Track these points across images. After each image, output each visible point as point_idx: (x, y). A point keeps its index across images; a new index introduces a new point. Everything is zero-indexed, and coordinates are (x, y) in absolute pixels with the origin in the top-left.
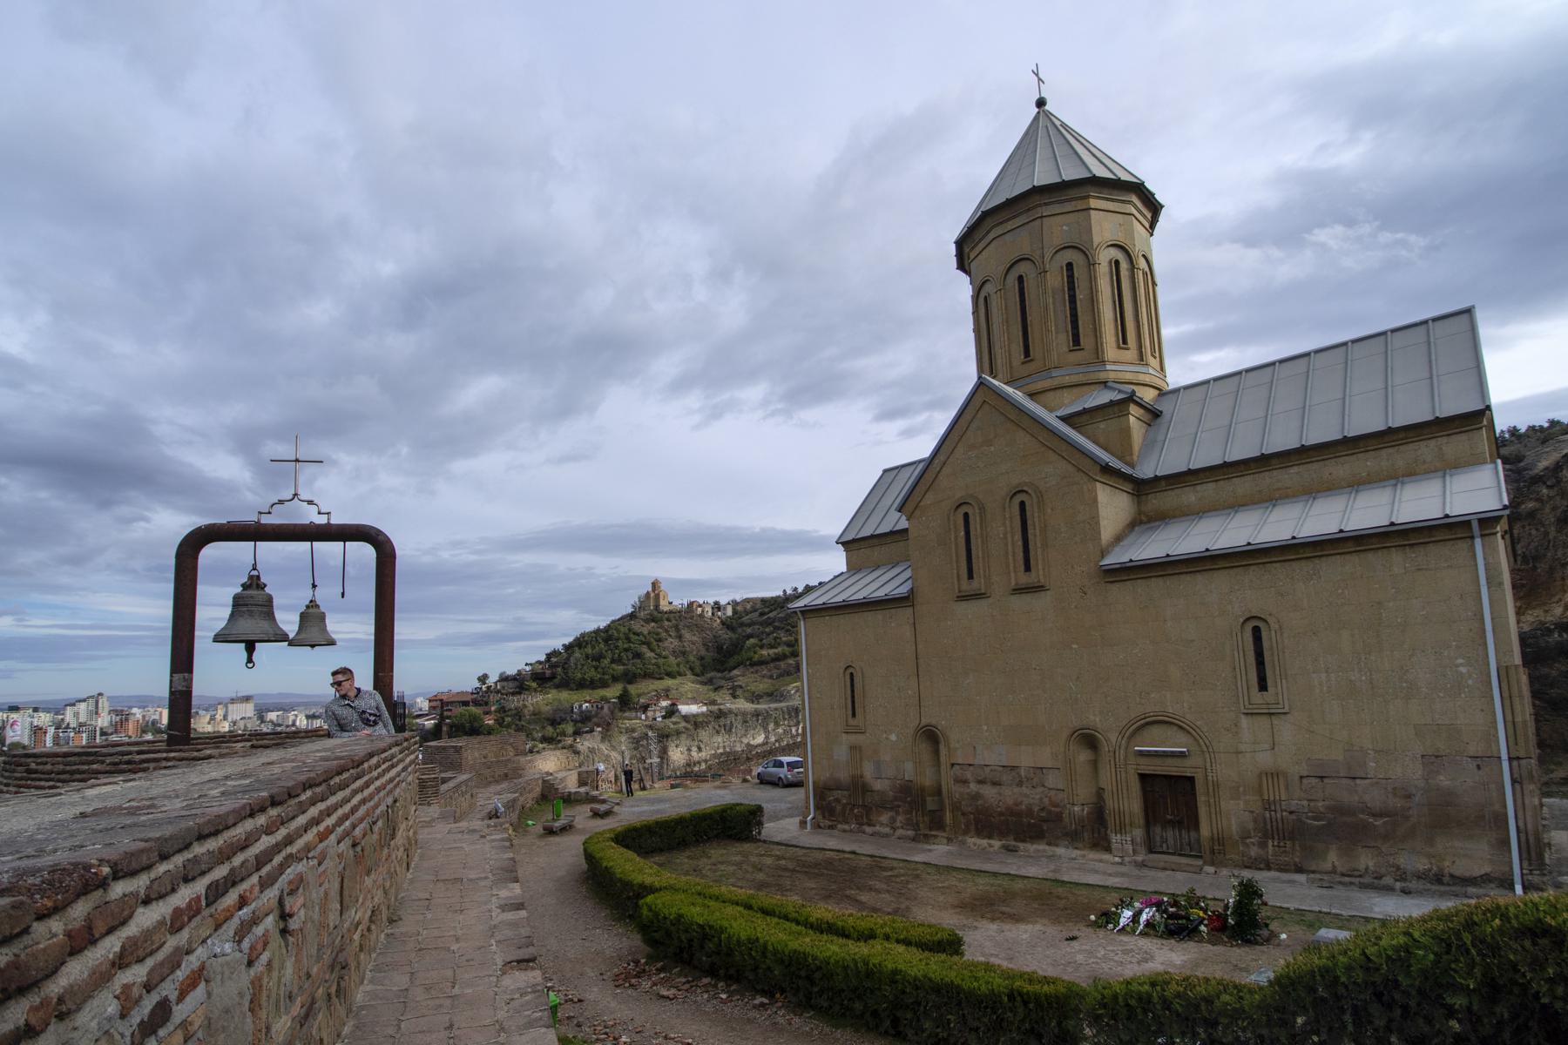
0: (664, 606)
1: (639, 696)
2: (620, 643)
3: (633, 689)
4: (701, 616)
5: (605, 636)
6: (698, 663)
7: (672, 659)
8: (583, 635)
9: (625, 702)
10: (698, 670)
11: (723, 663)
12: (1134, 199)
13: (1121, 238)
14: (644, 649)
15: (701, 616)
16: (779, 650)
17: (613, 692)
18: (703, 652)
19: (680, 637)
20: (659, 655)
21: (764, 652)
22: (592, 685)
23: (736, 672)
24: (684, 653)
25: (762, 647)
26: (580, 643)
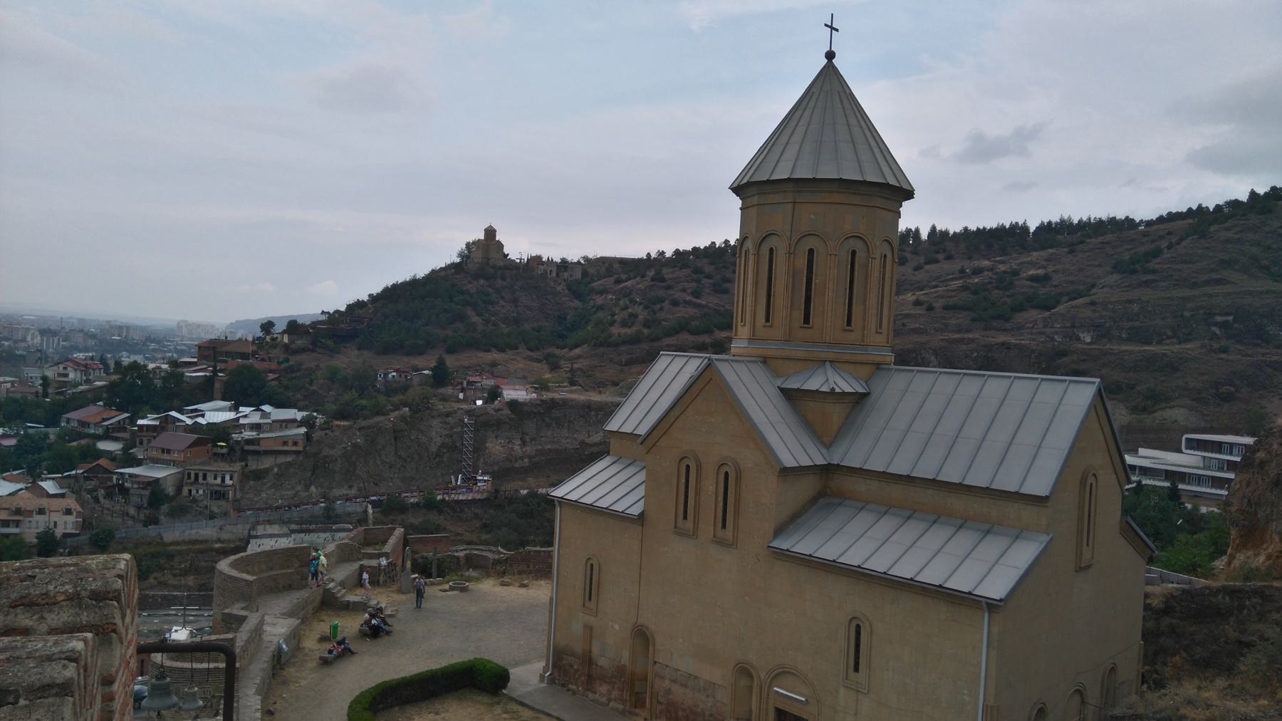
3: (451, 361)
9: (441, 377)
14: (470, 312)
15: (544, 276)
16: (634, 329)
19: (515, 301)
23: (577, 351)
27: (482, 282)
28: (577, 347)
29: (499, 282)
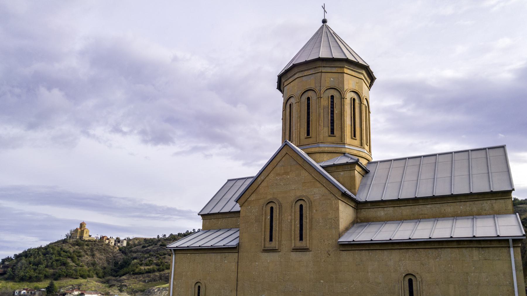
0: (86, 237)
1: (61, 288)
2: (54, 257)
3: (56, 284)
4: (108, 245)
5: (45, 251)
6: (101, 271)
7: (86, 267)
8: (29, 250)
10: (101, 275)
11: (116, 272)
12: (364, 72)
13: (356, 89)
14: (69, 260)
15: (108, 245)
16: (151, 267)
17: (43, 285)
18: (106, 265)
19: (93, 256)
20: (78, 265)
21: (142, 268)
22: (30, 279)
23: (124, 277)
24: (94, 264)
25: (141, 265)
26: (27, 254)
27: (77, 247)
28: (123, 275)
29: (86, 247)
